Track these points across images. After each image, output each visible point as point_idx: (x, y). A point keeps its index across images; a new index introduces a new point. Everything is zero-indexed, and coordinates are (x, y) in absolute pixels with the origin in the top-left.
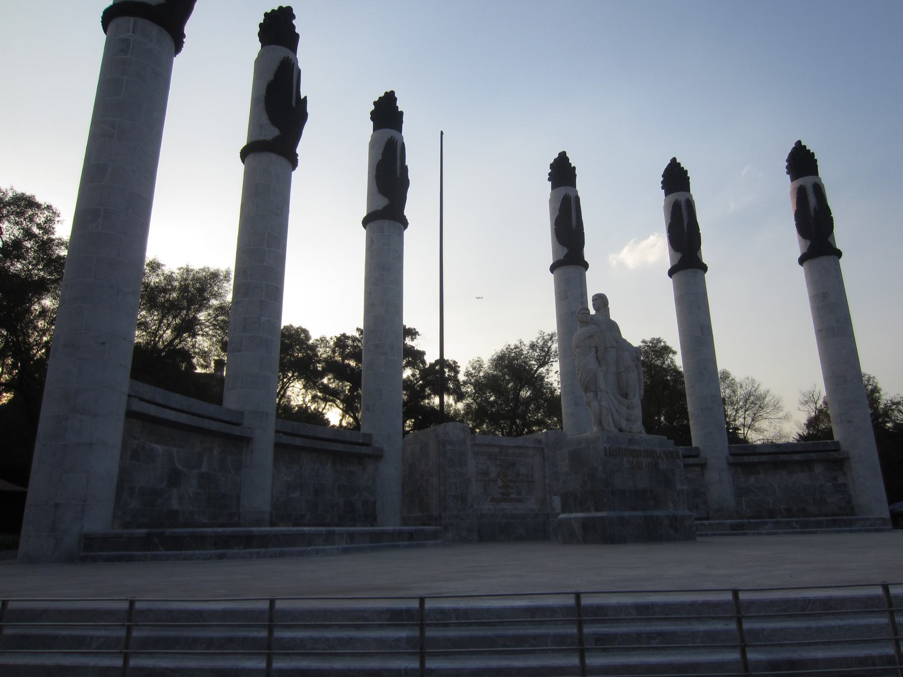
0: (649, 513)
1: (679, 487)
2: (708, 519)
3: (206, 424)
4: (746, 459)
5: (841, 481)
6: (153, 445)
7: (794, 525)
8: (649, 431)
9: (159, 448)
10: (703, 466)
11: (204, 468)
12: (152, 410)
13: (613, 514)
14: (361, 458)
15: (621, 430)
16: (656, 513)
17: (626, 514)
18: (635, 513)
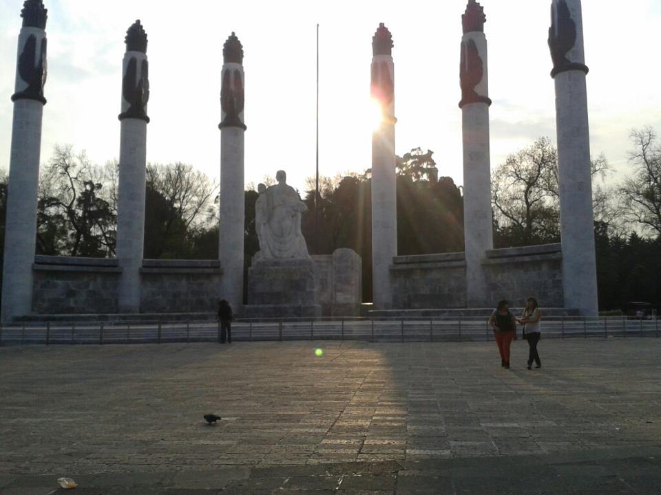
1: (308, 289)
2: (466, 307)
3: (85, 269)
5: (558, 278)
6: (56, 281)
7: (462, 313)
8: (311, 253)
9: (60, 282)
11: (91, 288)
12: (47, 267)
14: (209, 276)
15: (276, 257)
16: (285, 305)
17: (261, 306)
18: (268, 306)
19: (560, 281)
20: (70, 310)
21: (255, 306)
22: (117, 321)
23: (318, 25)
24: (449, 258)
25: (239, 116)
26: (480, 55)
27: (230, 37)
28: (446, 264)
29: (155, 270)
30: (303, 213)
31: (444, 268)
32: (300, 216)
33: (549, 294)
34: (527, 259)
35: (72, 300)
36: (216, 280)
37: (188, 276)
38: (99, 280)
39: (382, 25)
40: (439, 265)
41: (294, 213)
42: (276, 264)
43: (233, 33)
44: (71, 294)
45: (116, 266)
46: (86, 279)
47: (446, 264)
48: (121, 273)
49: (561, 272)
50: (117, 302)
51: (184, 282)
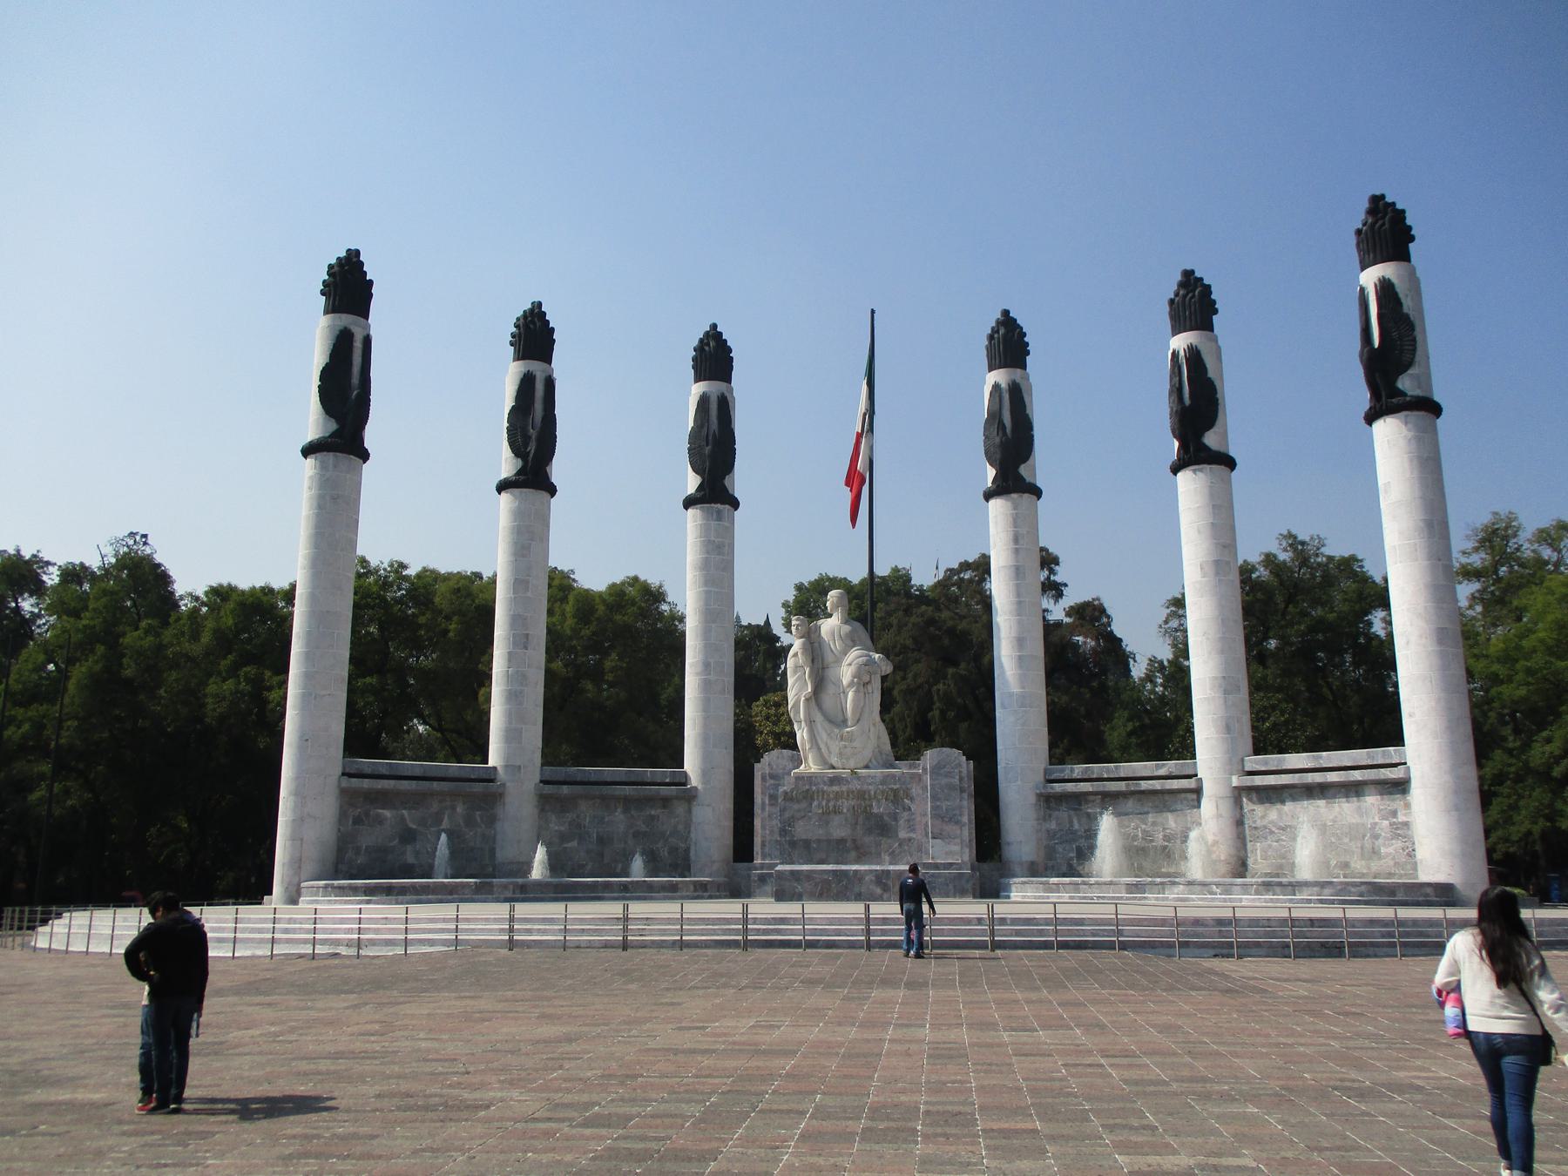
0: (844, 867)
1: (902, 834)
4: (1259, 781)
5: (1401, 818)
9: (387, 813)
10: (1198, 791)
19: (1406, 824)
20: (408, 872)
22: (509, 895)
23: (873, 312)
24: (1162, 772)
25: (727, 482)
26: (1211, 374)
27: (707, 334)
28: (1157, 785)
29: (565, 789)
30: (884, 679)
31: (1154, 792)
32: (877, 685)
33: (1383, 850)
34: (1333, 777)
35: (409, 848)
36: (680, 809)
37: (628, 803)
38: (459, 810)
39: (1006, 313)
40: (1145, 785)
41: (866, 678)
42: (835, 780)
43: (714, 326)
44: (408, 836)
45: (492, 781)
46: (435, 807)
47: (1157, 785)
48: (501, 795)
49: (1408, 806)
50: (492, 852)
51: (619, 816)
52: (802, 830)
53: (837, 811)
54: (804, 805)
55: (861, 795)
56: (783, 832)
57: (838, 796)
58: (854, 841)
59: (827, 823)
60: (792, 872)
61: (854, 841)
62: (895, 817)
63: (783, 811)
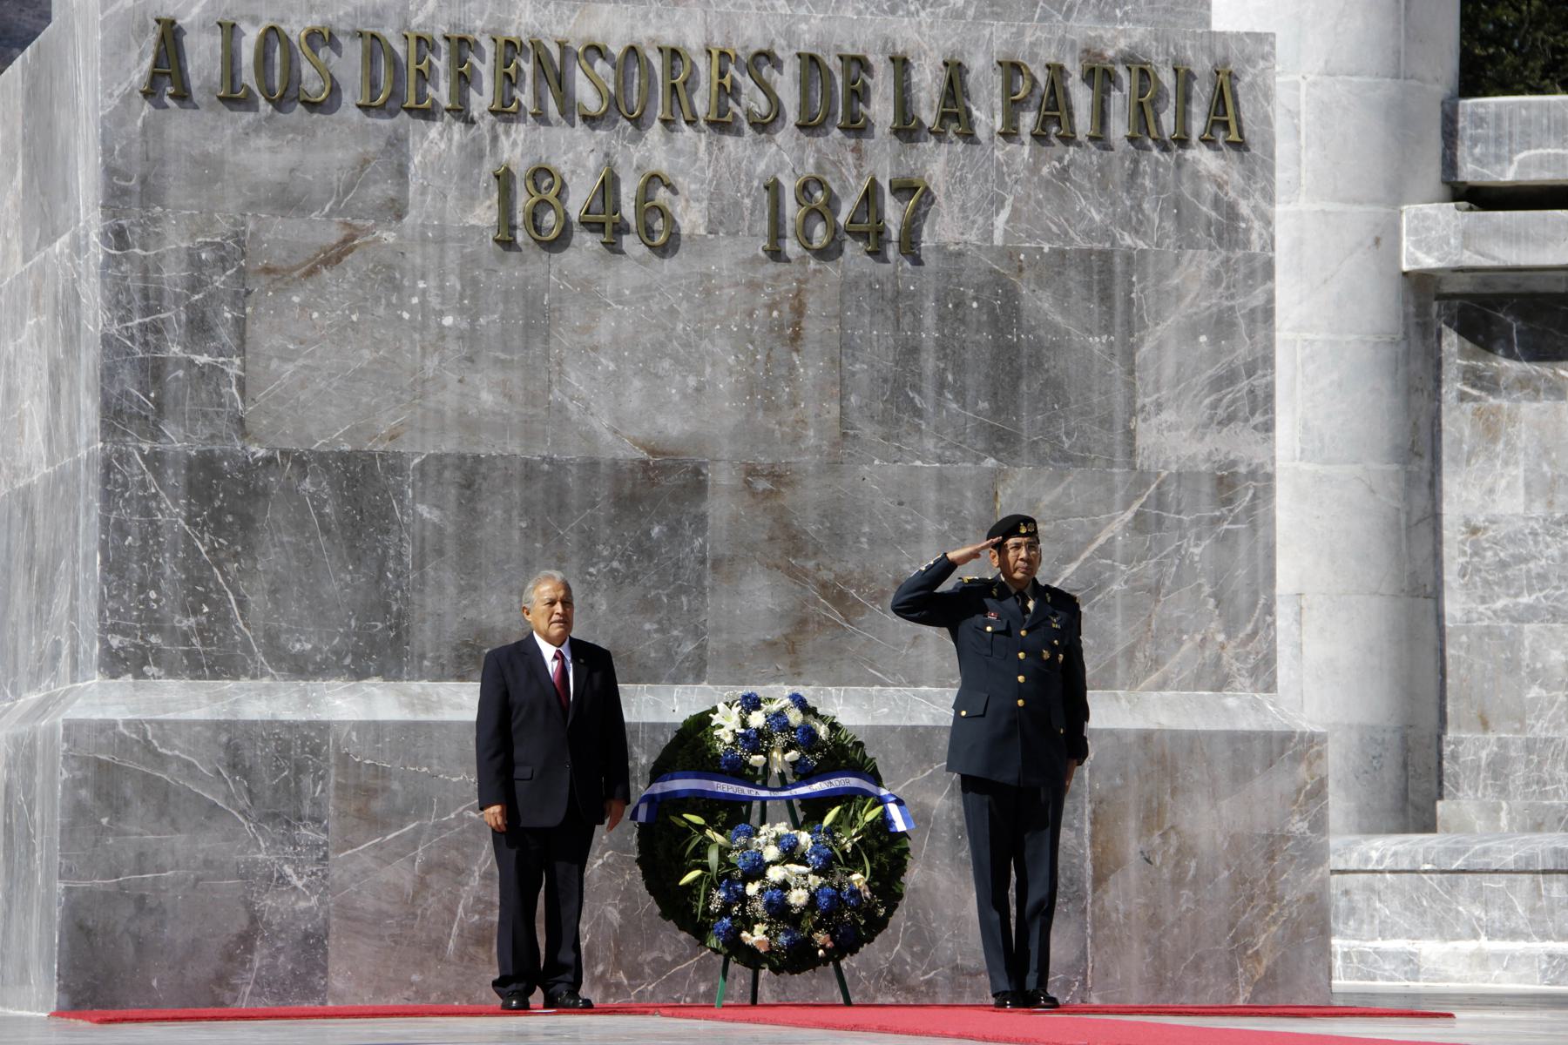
1: (1172, 439)
13: (184, 702)
17: (349, 704)
21: (265, 701)
52: (311, 379)
53: (628, 221)
54: (335, 146)
55: (836, 93)
56: (136, 393)
57: (647, 88)
58: (767, 482)
59: (537, 320)
60: (235, 746)
61: (767, 482)
62: (1104, 279)
63: (131, 195)
